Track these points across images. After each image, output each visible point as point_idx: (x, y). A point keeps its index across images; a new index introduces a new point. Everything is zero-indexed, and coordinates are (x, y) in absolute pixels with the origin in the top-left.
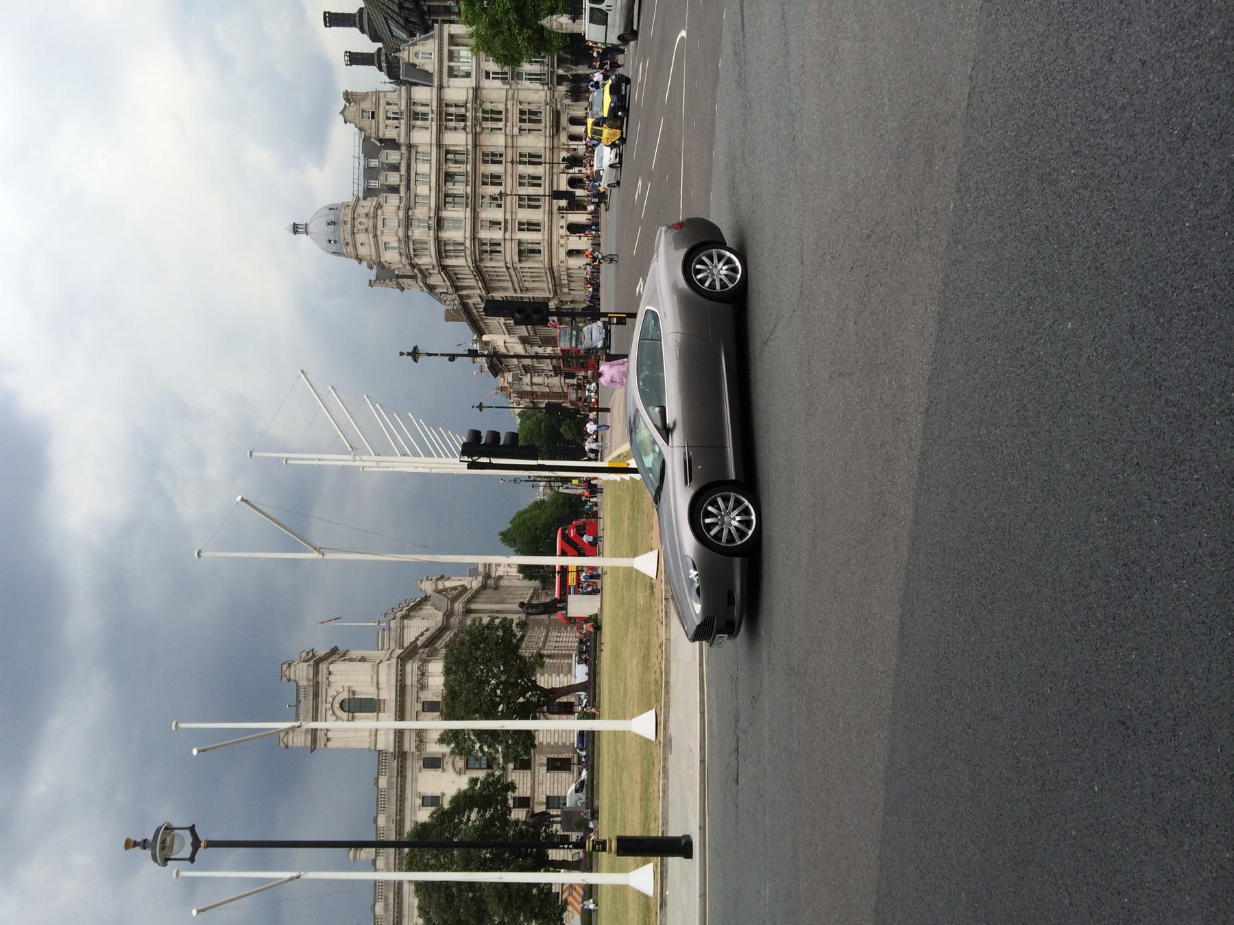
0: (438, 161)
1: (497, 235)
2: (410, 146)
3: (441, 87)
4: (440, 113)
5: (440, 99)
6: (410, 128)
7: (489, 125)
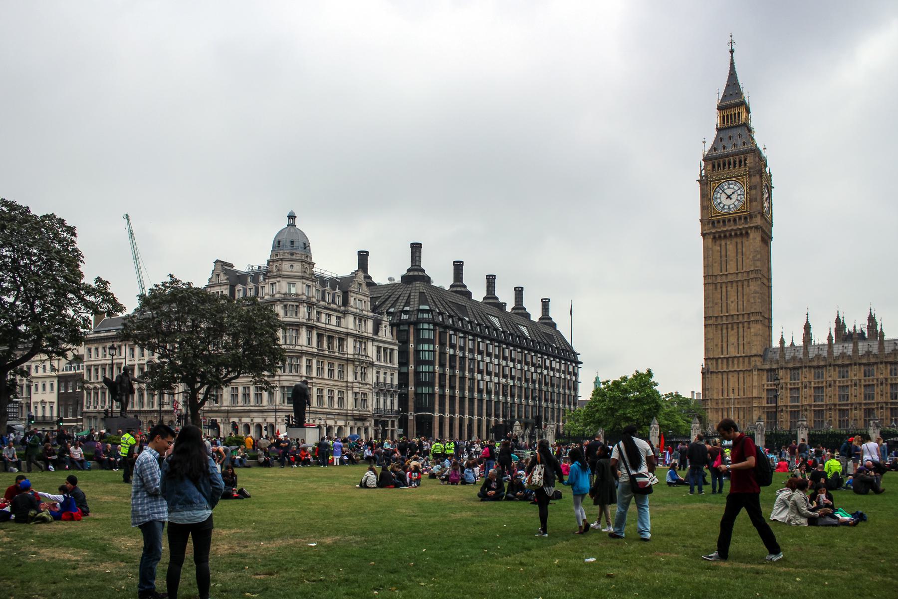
0: (340, 333)
1: (304, 371)
2: (345, 313)
3: (373, 340)
4: (362, 337)
5: (368, 338)
6: (355, 315)
7: (359, 371)
